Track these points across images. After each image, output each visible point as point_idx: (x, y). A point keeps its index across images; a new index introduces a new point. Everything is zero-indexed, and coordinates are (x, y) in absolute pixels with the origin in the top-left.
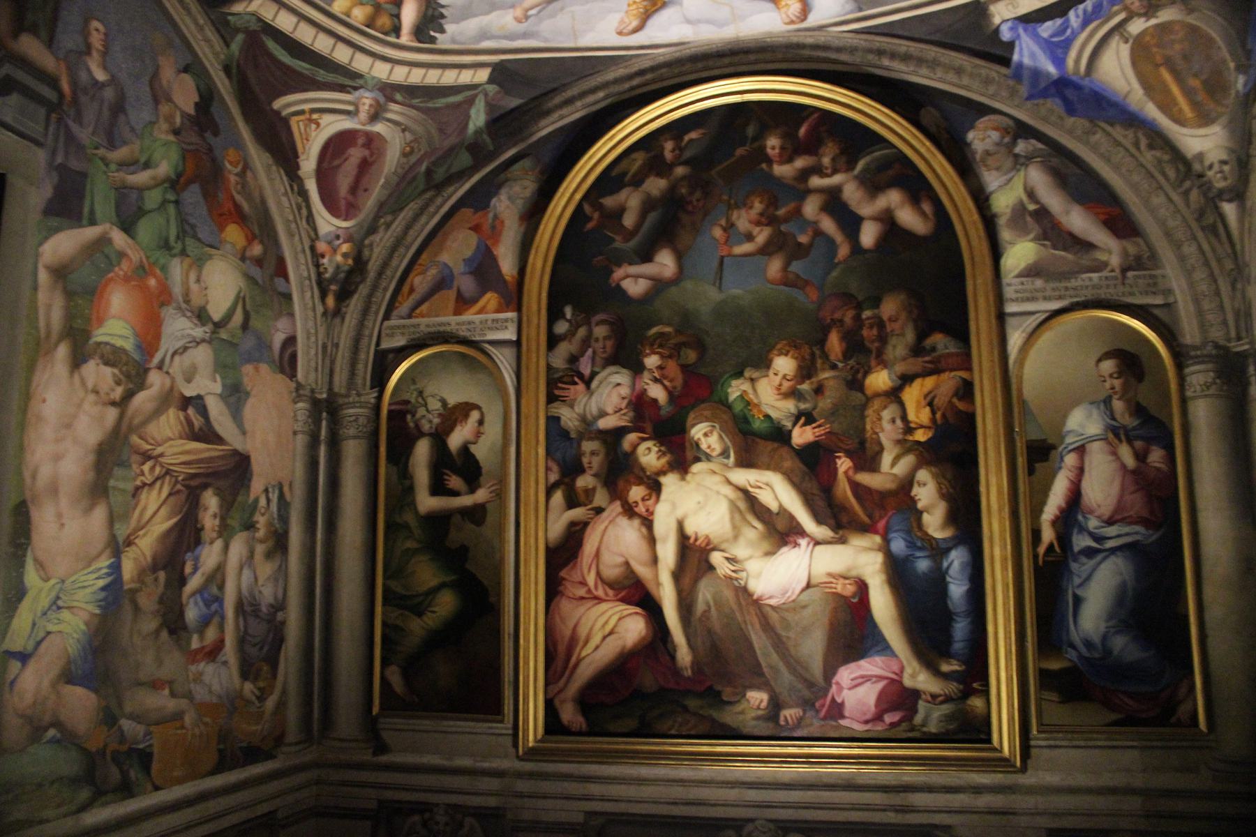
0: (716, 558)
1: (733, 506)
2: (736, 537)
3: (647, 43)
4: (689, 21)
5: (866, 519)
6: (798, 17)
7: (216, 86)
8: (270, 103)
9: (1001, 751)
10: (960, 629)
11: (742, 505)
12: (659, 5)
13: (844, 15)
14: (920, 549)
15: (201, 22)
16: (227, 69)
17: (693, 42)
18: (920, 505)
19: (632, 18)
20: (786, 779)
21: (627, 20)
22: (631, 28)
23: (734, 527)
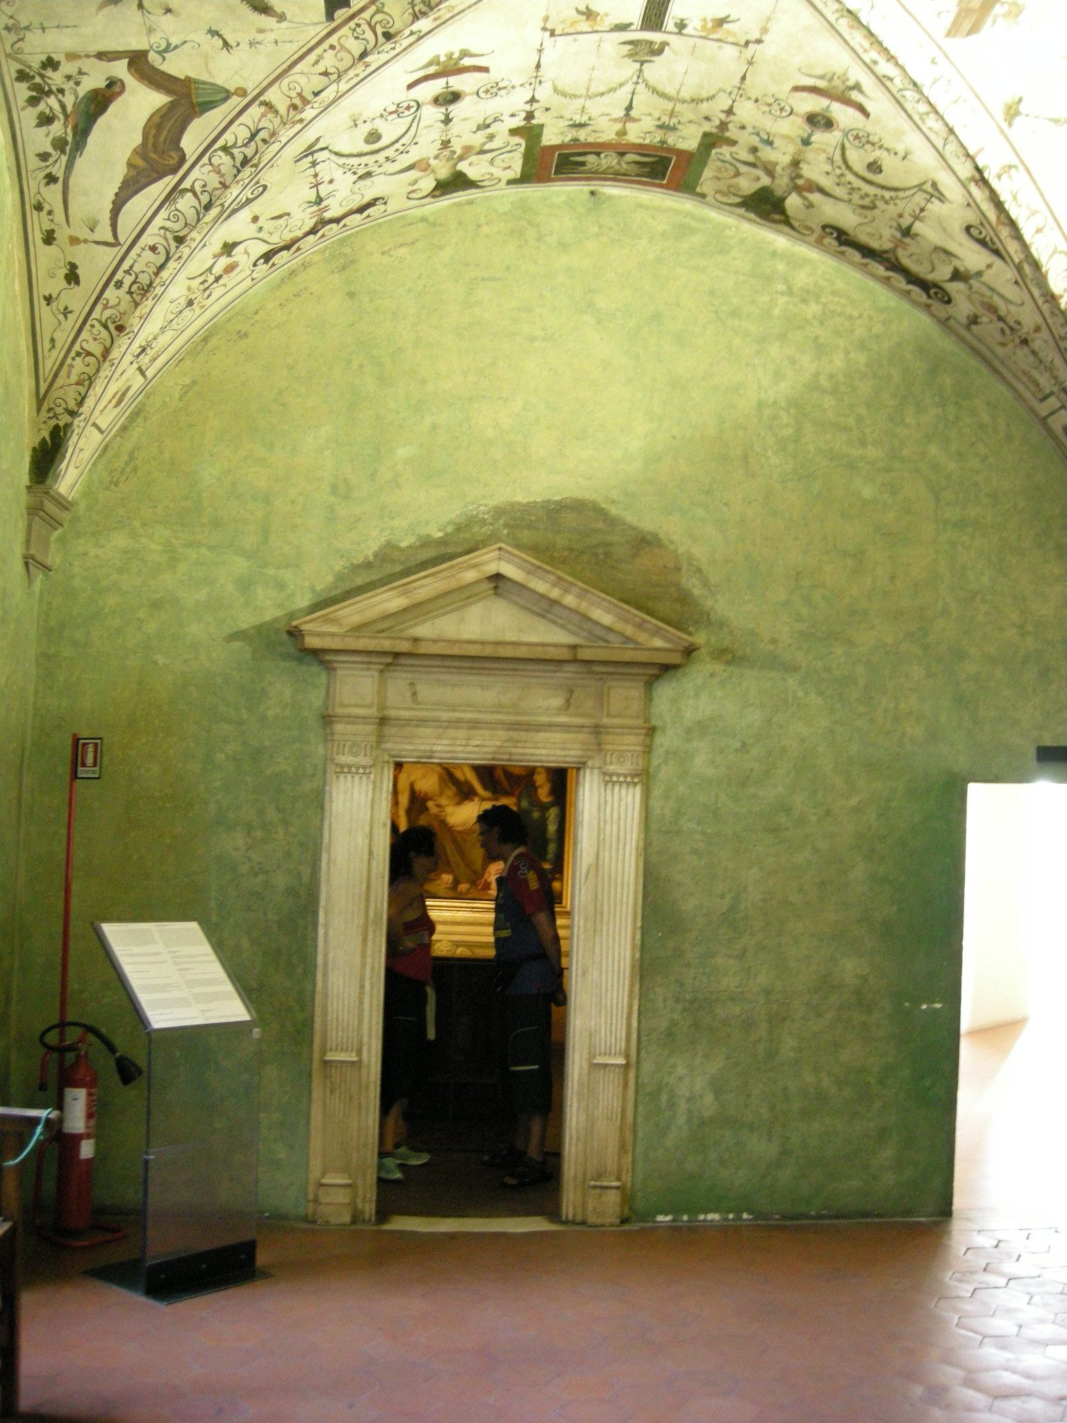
0: (430, 804)
1: (441, 778)
2: (442, 793)
5: (509, 789)
9: (565, 907)
10: (552, 847)
11: (446, 777)
14: (536, 806)
18: (537, 784)
20: (459, 920)
23: (440, 787)
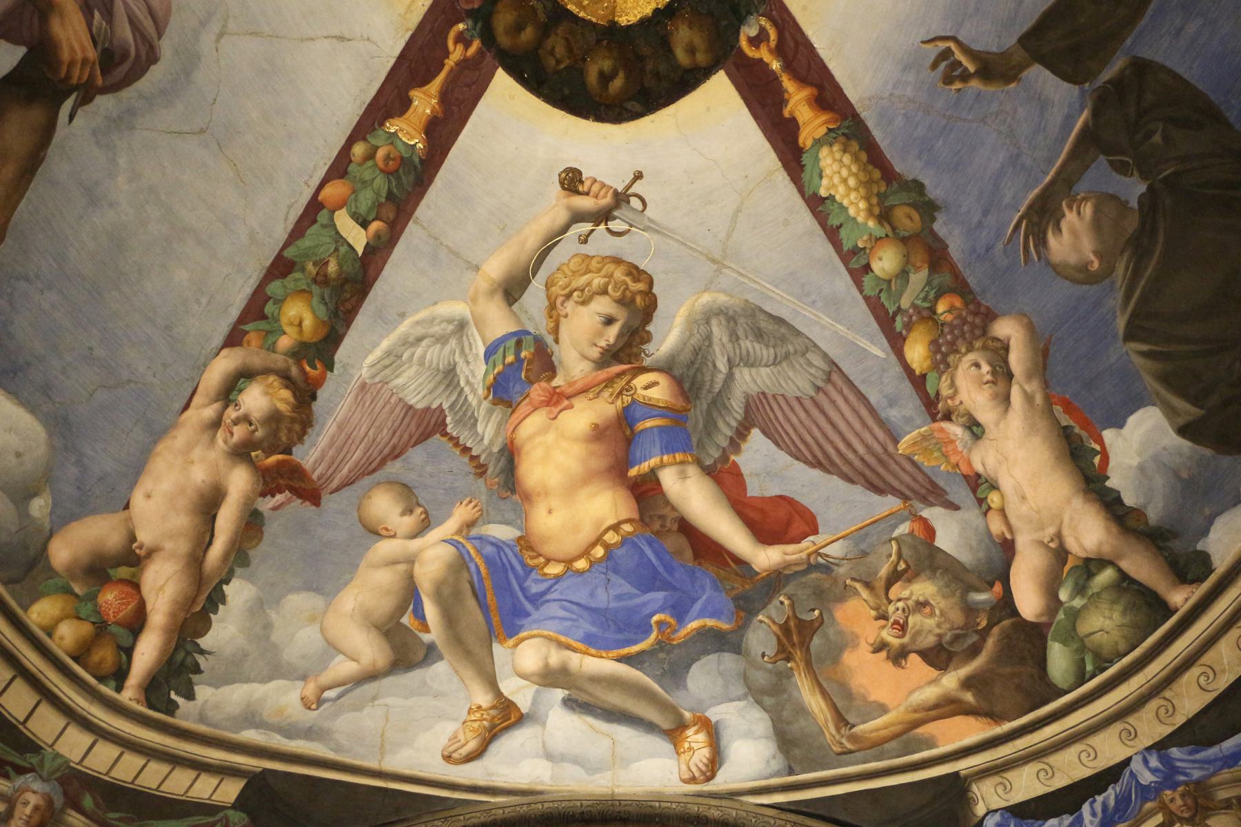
3: (482, 782)
4: (549, 756)
6: (703, 773)
12: (513, 720)
13: (767, 778)
17: (549, 792)
19: (470, 735)
21: (461, 737)
22: (464, 751)
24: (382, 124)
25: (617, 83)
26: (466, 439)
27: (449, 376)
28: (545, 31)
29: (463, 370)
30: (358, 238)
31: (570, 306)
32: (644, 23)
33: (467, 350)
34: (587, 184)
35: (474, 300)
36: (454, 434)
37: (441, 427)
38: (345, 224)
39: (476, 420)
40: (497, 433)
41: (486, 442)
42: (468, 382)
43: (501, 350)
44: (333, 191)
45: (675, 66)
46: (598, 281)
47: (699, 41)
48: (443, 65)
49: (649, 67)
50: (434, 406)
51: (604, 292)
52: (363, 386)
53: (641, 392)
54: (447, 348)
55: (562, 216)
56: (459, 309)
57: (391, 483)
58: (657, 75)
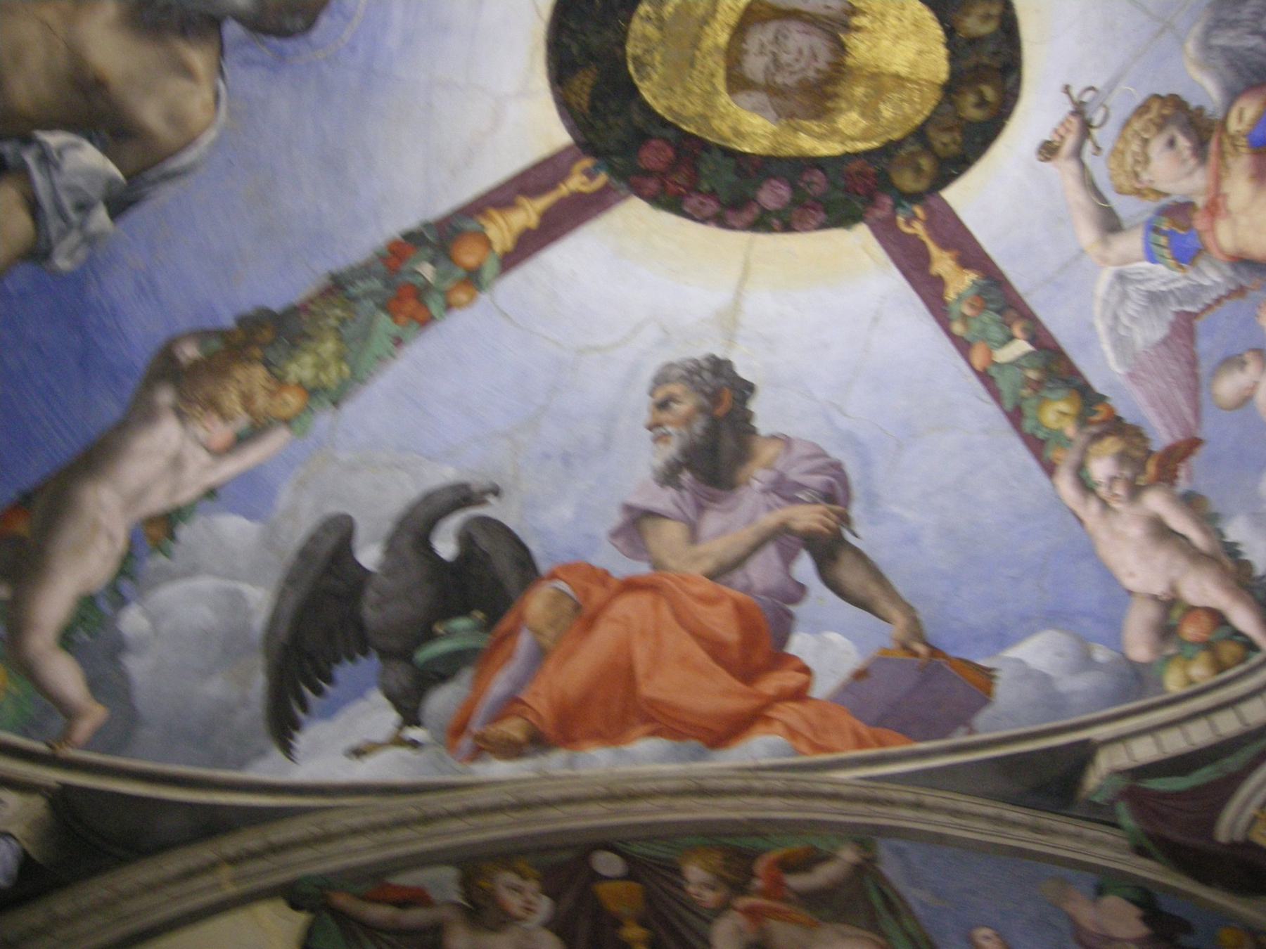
7: (1145, 879)
8: (1211, 839)
15: (1071, 828)
16: (1140, 851)
24: (945, 303)
25: (989, 93)
26: (1208, 298)
27: (1155, 299)
28: (928, 147)
29: (1156, 286)
30: (1021, 347)
31: (1145, 177)
32: (953, 58)
33: (1140, 277)
34: (1057, 139)
35: (1105, 261)
36: (1201, 306)
37: (1190, 317)
38: (1006, 354)
39: (1201, 286)
40: (1218, 269)
41: (1219, 280)
42: (1165, 284)
43: (1155, 248)
44: (978, 359)
45: (993, 36)
46: (1135, 146)
47: (980, 10)
48: (923, 243)
49: (986, 60)
50: (1171, 317)
51: (1146, 142)
52: (1131, 376)
53: (1240, 128)
54: (1134, 295)
55: (1072, 166)
56: (1107, 275)
57: (1215, 373)
58: (995, 54)
